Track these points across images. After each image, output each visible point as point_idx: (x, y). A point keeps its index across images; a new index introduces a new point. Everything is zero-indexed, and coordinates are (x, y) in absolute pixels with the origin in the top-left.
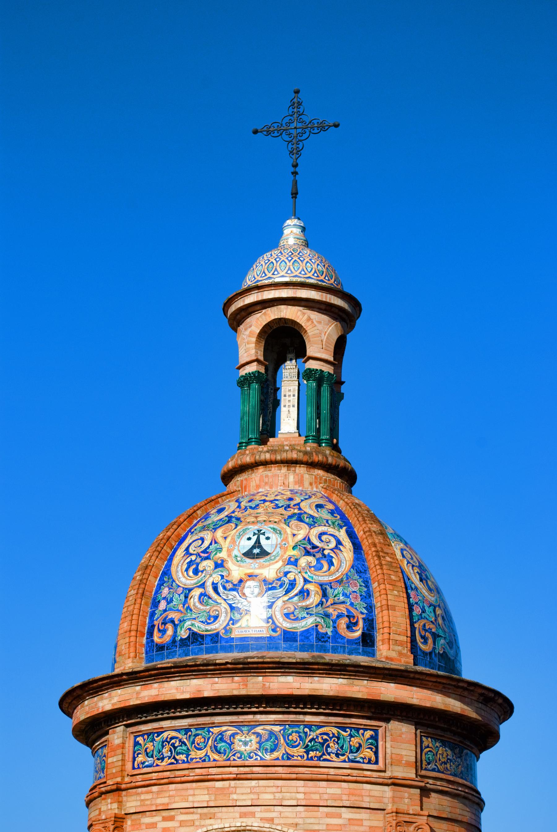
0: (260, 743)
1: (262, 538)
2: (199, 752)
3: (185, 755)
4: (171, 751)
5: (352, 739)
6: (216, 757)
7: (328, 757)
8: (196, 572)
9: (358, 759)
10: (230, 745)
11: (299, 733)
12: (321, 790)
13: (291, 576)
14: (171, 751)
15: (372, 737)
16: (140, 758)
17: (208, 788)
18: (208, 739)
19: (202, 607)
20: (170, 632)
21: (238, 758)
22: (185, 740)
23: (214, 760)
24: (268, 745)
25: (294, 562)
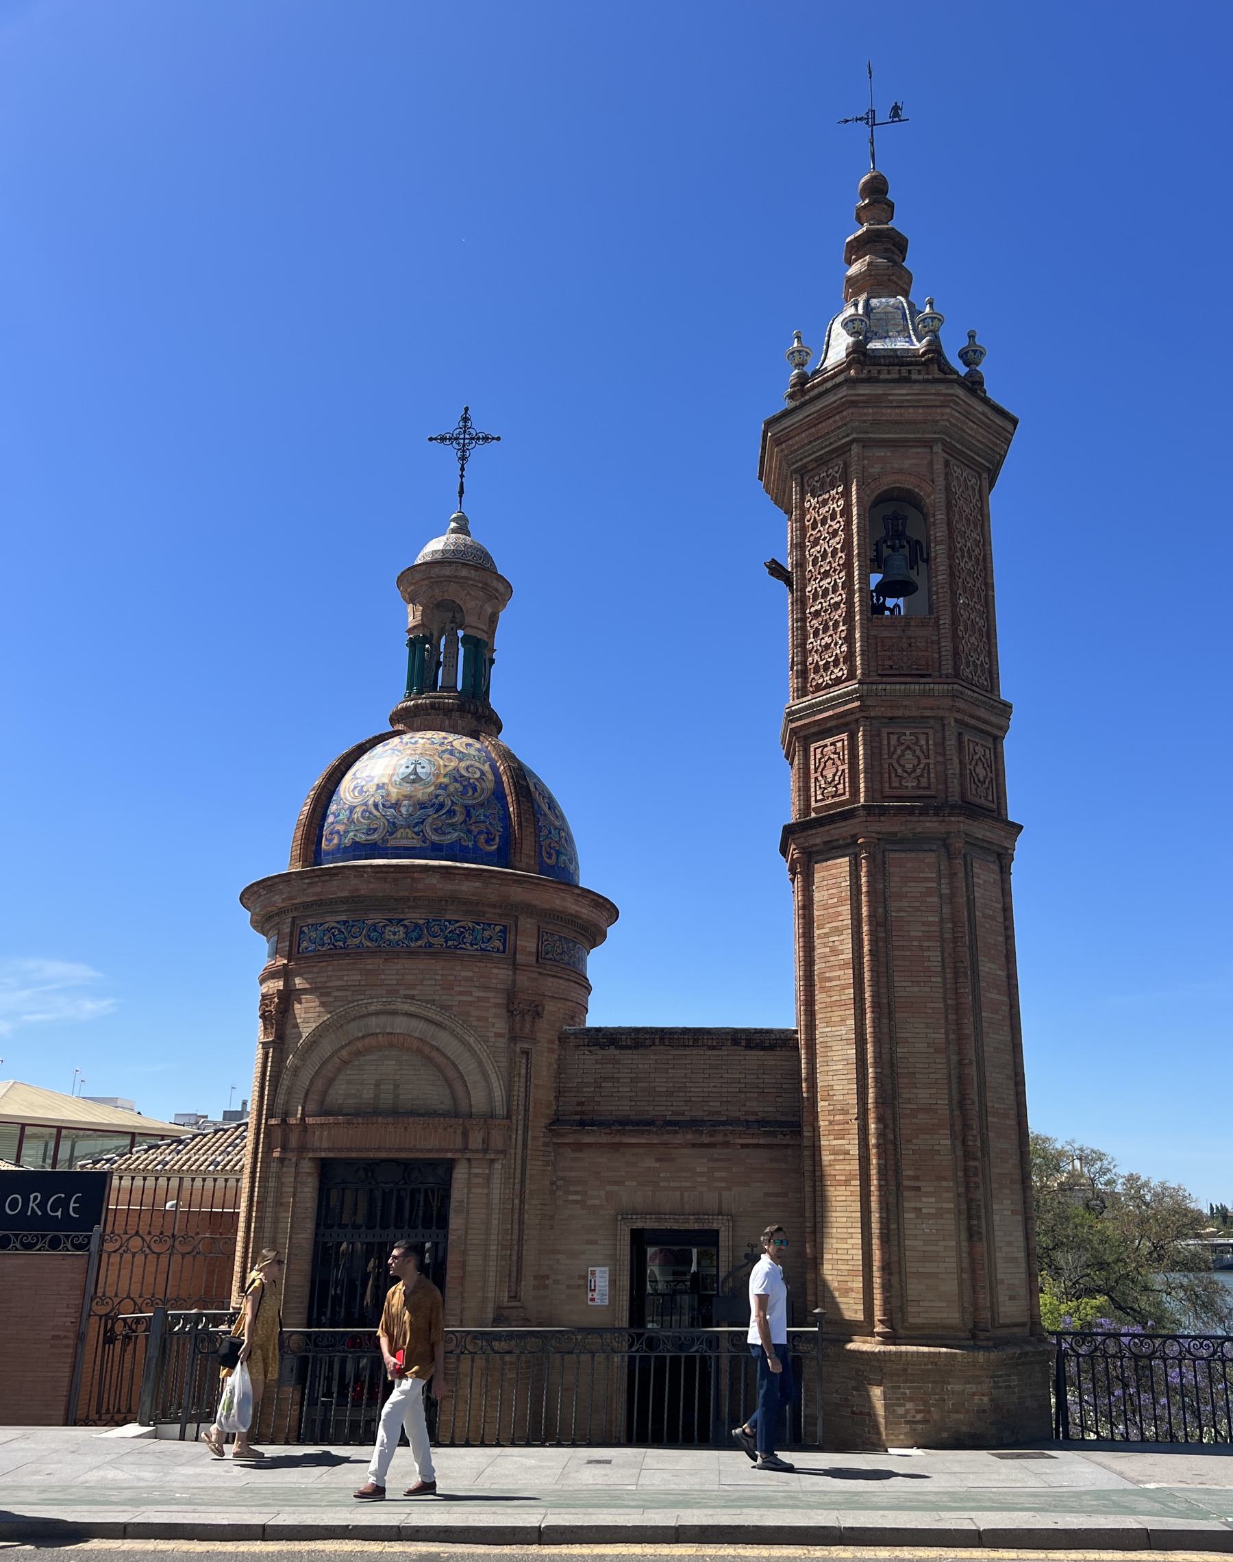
0: (406, 933)
1: (419, 770)
13: (441, 799)
20: (335, 841)
24: (414, 935)
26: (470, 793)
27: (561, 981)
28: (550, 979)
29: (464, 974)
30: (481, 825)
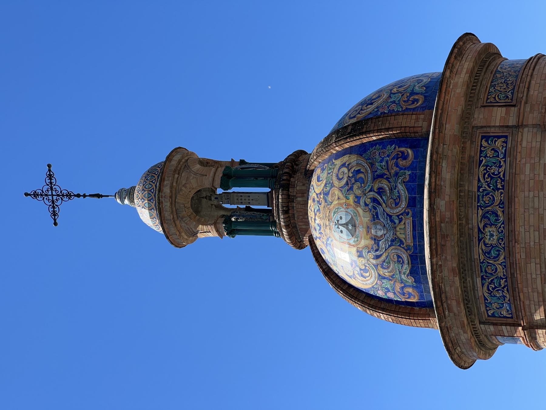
0: (491, 225)
4: (498, 290)
5: (488, 155)
7: (502, 174)
9: (503, 151)
10: (493, 247)
11: (483, 196)
13: (368, 201)
14: (498, 290)
15: (487, 141)
16: (504, 313)
18: (488, 262)
19: (391, 267)
21: (503, 241)
23: (504, 258)
24: (493, 218)
26: (361, 175)
27: (533, 82)
28: (531, 92)
29: (527, 172)
30: (390, 164)
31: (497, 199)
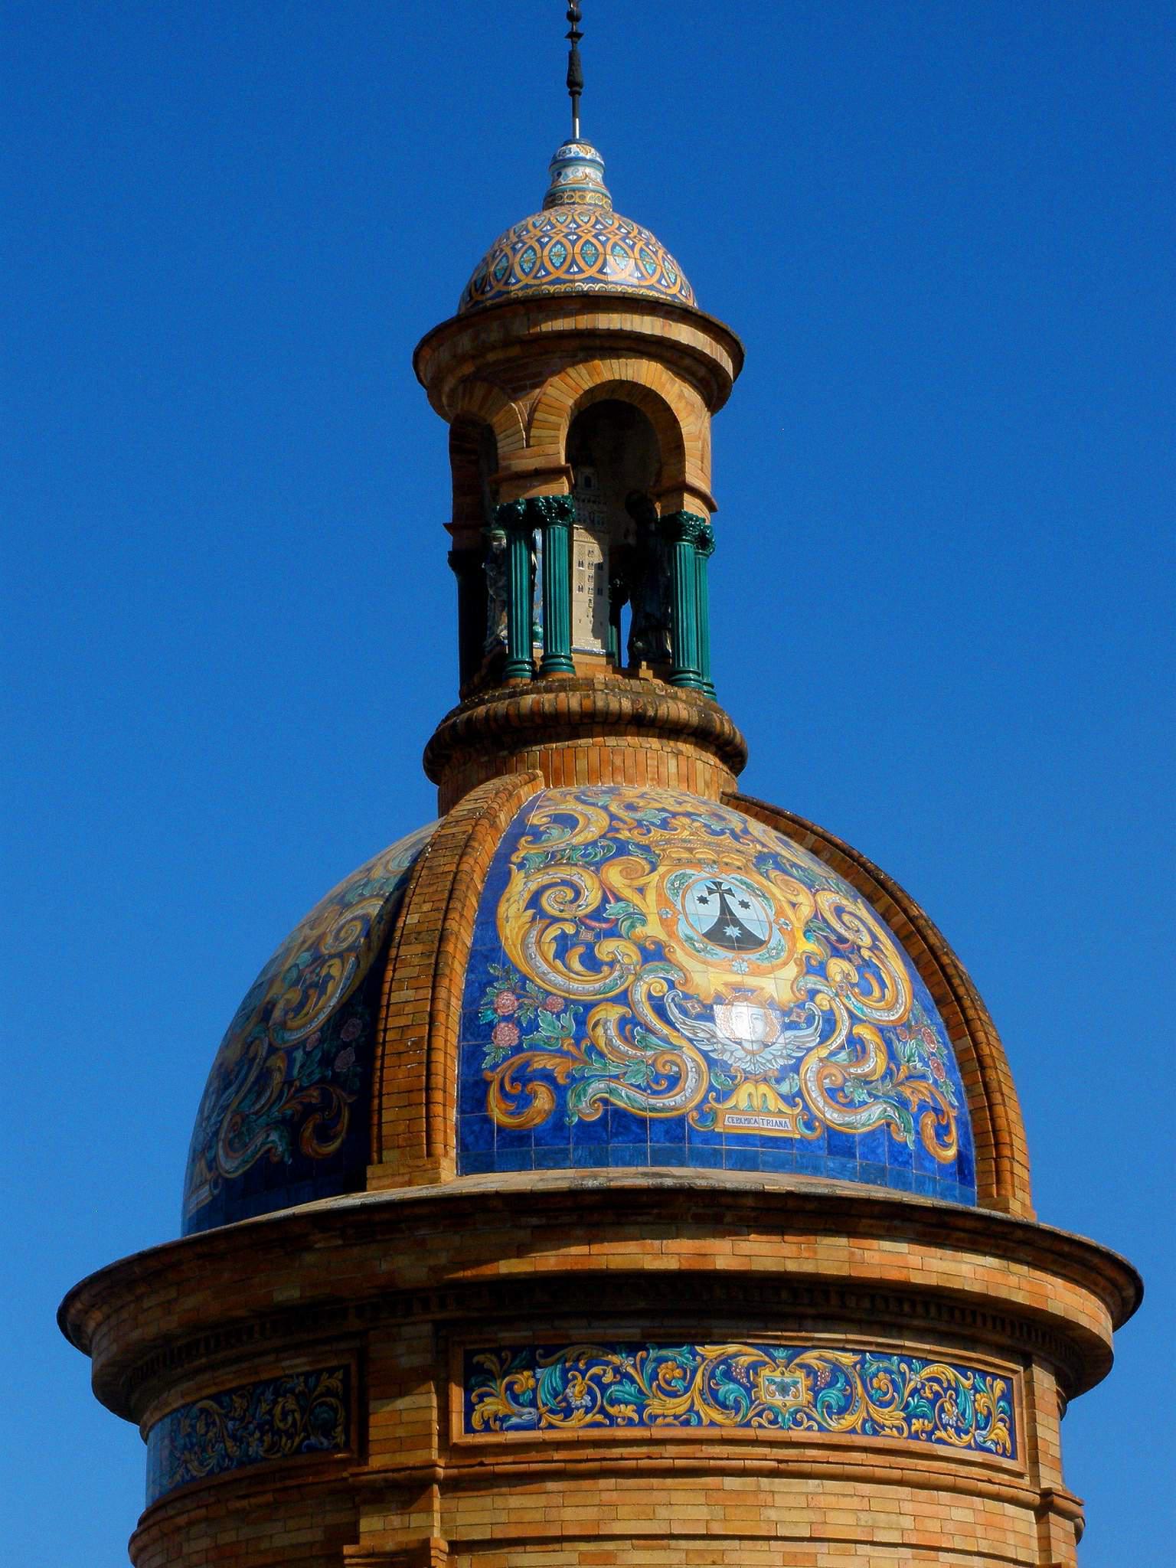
0: (815, 1390)
2: (671, 1402)
3: (631, 1407)
4: (590, 1392)
5: (978, 1396)
6: (718, 1417)
8: (592, 963)
9: (989, 1444)
10: (748, 1390)
11: (890, 1372)
12: (943, 1512)
14: (590, 1392)
17: (707, 1490)
18: (694, 1372)
19: (632, 1052)
20: (543, 1101)
21: (771, 1422)
22: (631, 1370)
23: (712, 1424)
24: (833, 1396)
25: (821, 971)
26: (877, 993)
31: (890, 1416)
